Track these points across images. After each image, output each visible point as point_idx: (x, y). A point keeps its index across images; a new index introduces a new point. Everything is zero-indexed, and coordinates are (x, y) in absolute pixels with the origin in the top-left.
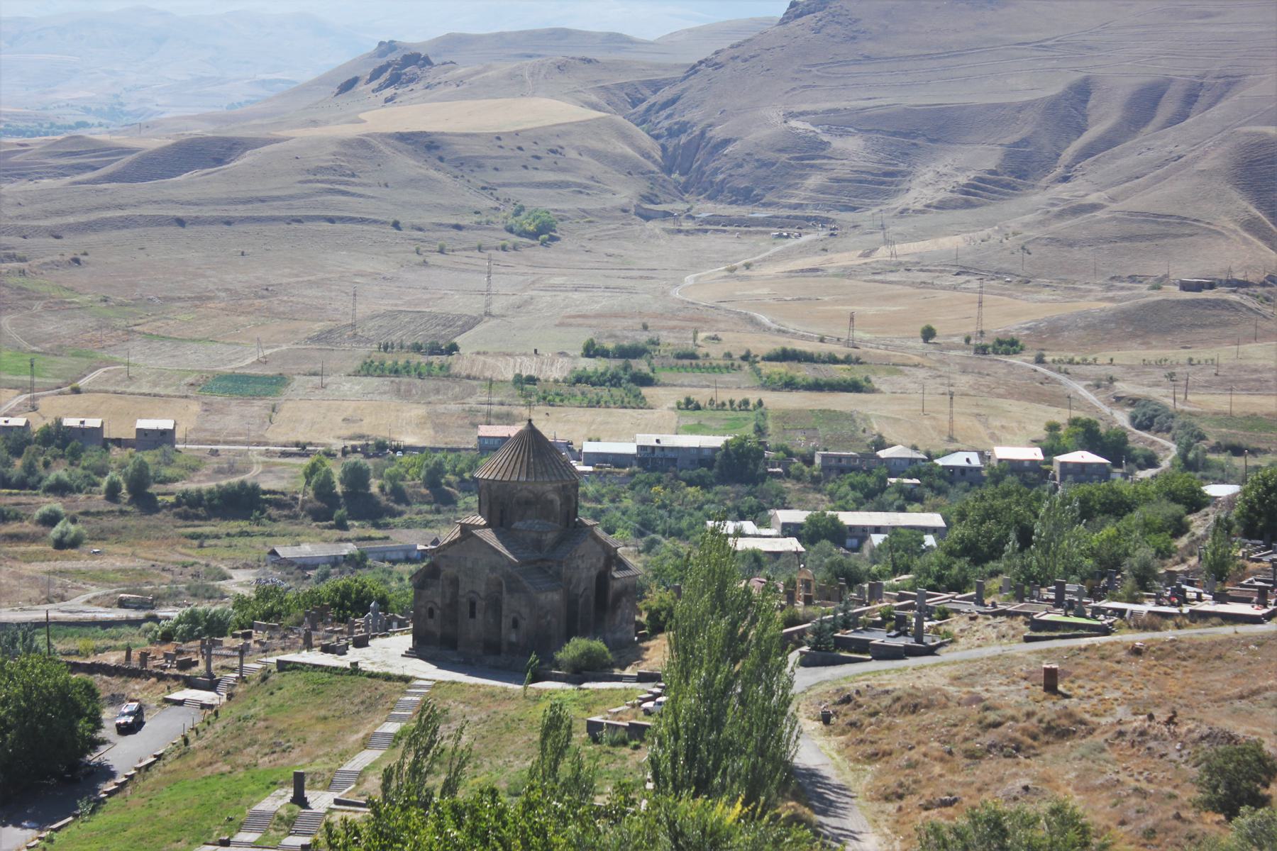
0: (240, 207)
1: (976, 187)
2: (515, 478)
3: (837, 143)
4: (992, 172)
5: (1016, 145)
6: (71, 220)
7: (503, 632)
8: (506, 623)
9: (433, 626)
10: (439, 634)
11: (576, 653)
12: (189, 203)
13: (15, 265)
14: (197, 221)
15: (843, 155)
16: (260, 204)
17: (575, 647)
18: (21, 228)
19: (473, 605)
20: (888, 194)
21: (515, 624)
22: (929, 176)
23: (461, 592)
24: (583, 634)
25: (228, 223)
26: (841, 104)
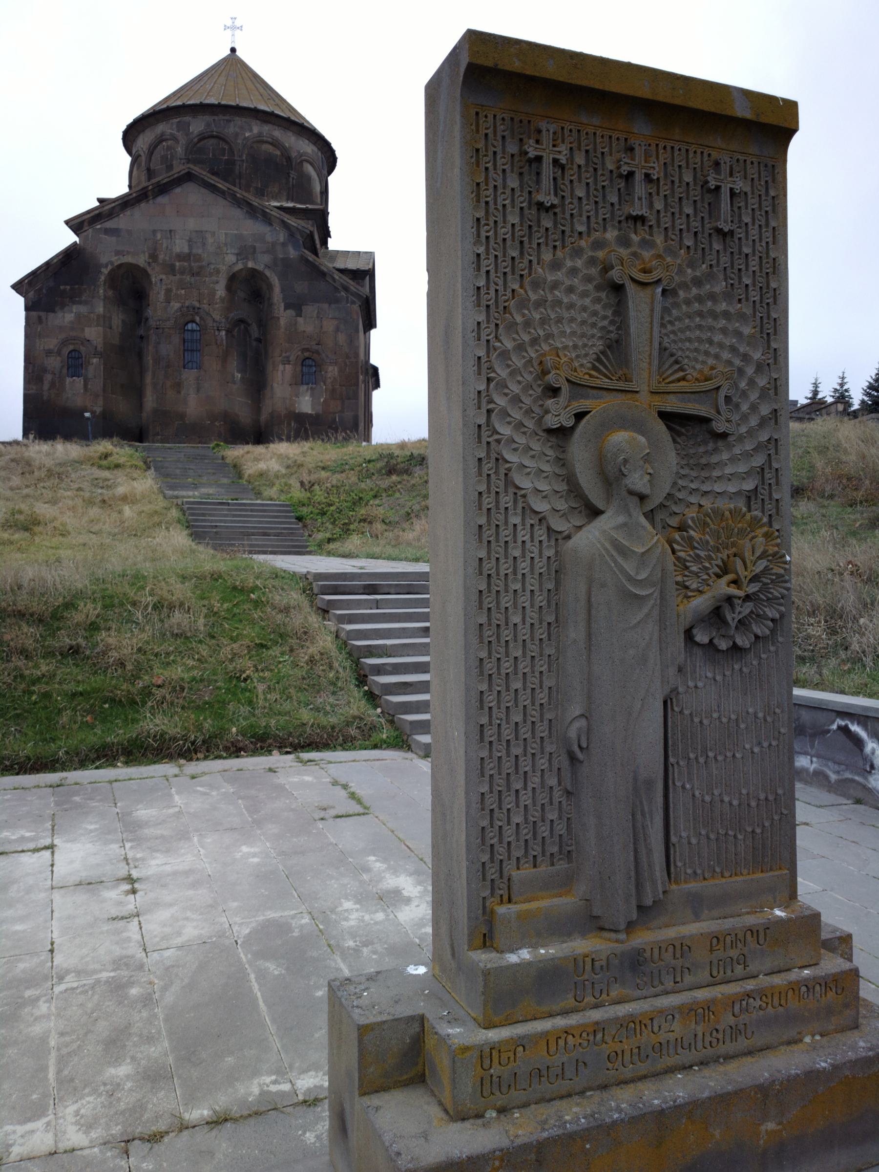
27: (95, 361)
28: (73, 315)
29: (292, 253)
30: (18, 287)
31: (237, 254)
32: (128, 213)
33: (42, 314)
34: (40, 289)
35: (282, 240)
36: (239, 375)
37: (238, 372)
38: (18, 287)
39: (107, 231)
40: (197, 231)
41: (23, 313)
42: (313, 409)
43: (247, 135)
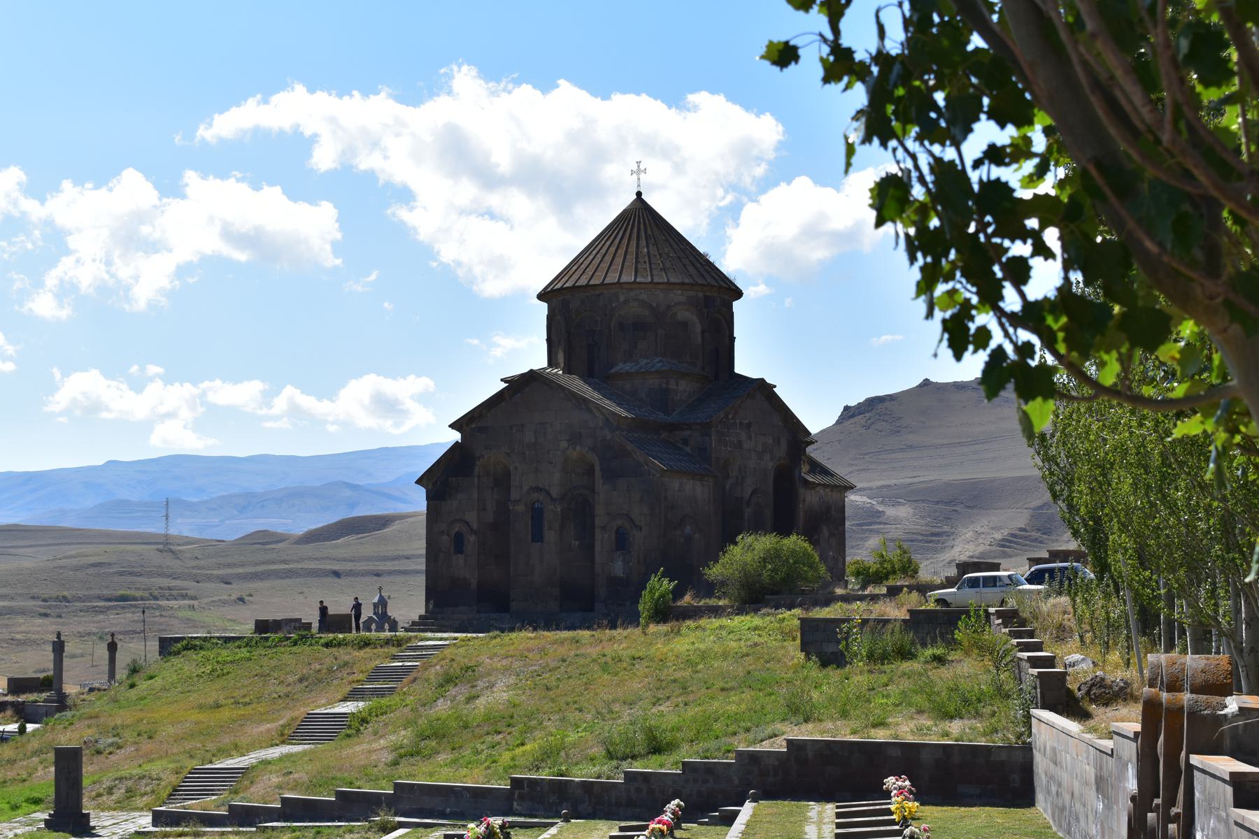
0: (389, 563)
1: (1010, 542)
2: (612, 278)
3: (890, 512)
4: (1021, 529)
5: (1040, 507)
6: (241, 570)
7: (598, 559)
8: (603, 541)
9: (464, 568)
10: (474, 583)
11: (749, 557)
12: (344, 560)
13: (187, 602)
14: (351, 573)
15: (896, 521)
16: (406, 561)
17: (749, 551)
18: (195, 575)
19: (537, 515)
20: (936, 551)
21: (621, 542)
22: (969, 535)
23: (514, 495)
24: (757, 527)
25: (378, 575)
26: (892, 482)
27: (472, 538)
30: (419, 482)
38: (419, 482)
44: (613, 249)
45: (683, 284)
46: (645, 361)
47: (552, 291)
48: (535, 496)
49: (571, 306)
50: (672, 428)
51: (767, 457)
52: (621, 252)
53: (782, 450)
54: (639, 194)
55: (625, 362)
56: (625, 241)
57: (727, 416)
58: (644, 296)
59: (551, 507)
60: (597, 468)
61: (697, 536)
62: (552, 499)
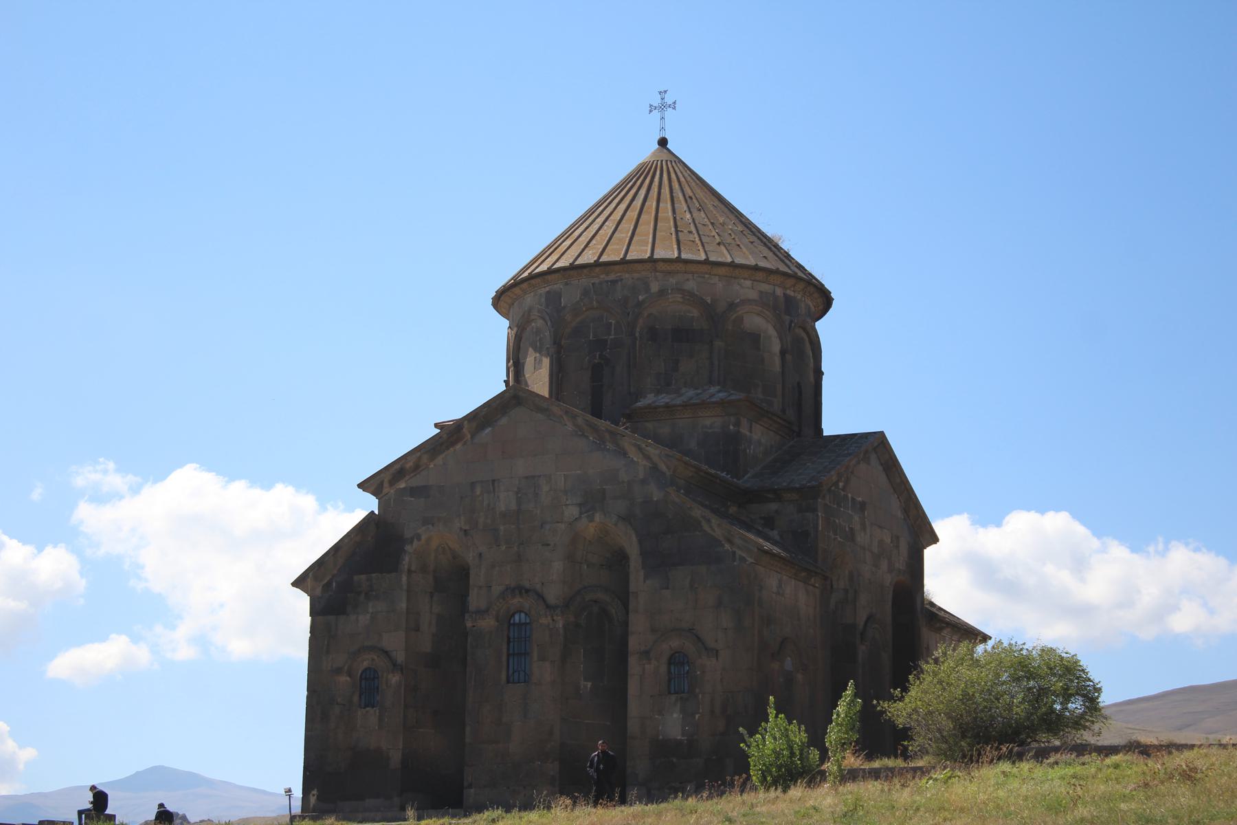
2: (640, 251)
7: (635, 708)
8: (642, 679)
9: (379, 731)
10: (396, 757)
21: (680, 676)
23: (476, 600)
27: (395, 679)
28: (368, 616)
29: (657, 495)
30: (298, 583)
31: (580, 505)
32: (439, 460)
33: (332, 618)
34: (329, 584)
35: (641, 476)
36: (589, 685)
37: (586, 680)
38: (298, 583)
39: (414, 491)
40: (527, 478)
41: (307, 620)
42: (683, 735)
43: (641, 298)
44: (633, 214)
45: (756, 268)
46: (691, 393)
47: (532, 277)
48: (516, 601)
49: (558, 310)
50: (748, 497)
51: (884, 565)
52: (648, 218)
53: (901, 561)
54: (663, 142)
55: (658, 392)
56: (652, 203)
57: (836, 484)
58: (691, 285)
59: (544, 621)
60: (633, 551)
61: (800, 677)
62: (548, 606)
